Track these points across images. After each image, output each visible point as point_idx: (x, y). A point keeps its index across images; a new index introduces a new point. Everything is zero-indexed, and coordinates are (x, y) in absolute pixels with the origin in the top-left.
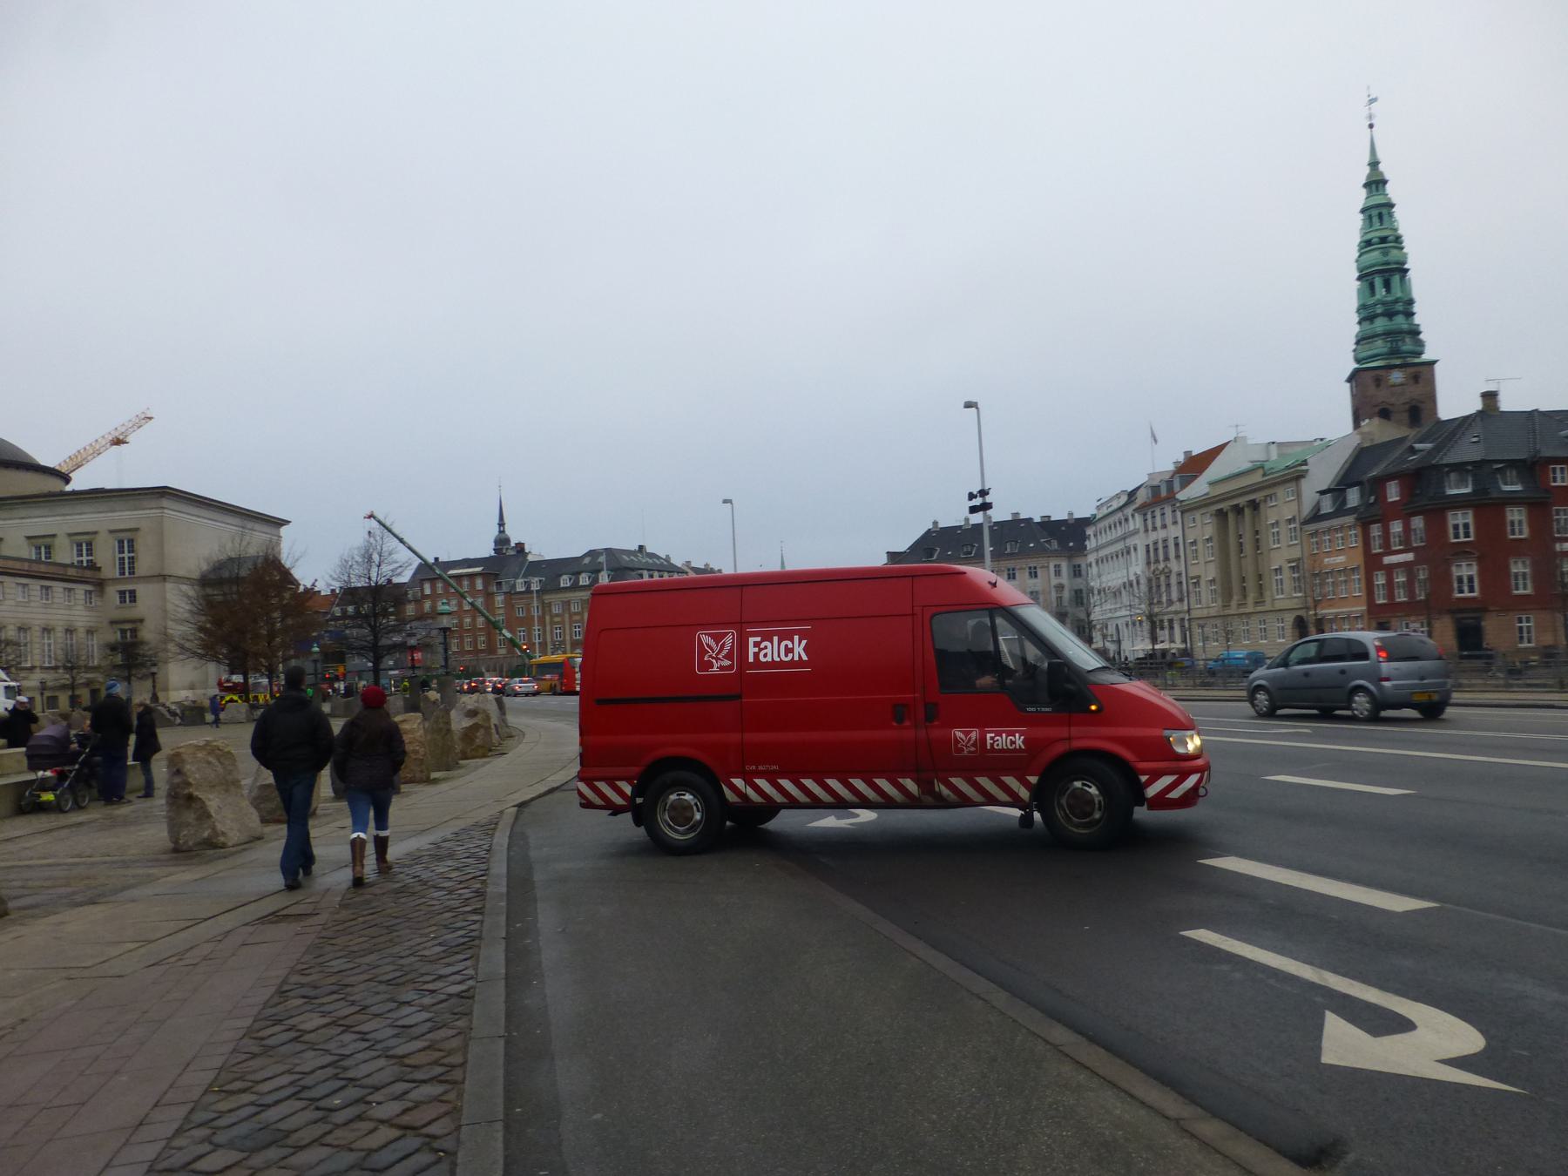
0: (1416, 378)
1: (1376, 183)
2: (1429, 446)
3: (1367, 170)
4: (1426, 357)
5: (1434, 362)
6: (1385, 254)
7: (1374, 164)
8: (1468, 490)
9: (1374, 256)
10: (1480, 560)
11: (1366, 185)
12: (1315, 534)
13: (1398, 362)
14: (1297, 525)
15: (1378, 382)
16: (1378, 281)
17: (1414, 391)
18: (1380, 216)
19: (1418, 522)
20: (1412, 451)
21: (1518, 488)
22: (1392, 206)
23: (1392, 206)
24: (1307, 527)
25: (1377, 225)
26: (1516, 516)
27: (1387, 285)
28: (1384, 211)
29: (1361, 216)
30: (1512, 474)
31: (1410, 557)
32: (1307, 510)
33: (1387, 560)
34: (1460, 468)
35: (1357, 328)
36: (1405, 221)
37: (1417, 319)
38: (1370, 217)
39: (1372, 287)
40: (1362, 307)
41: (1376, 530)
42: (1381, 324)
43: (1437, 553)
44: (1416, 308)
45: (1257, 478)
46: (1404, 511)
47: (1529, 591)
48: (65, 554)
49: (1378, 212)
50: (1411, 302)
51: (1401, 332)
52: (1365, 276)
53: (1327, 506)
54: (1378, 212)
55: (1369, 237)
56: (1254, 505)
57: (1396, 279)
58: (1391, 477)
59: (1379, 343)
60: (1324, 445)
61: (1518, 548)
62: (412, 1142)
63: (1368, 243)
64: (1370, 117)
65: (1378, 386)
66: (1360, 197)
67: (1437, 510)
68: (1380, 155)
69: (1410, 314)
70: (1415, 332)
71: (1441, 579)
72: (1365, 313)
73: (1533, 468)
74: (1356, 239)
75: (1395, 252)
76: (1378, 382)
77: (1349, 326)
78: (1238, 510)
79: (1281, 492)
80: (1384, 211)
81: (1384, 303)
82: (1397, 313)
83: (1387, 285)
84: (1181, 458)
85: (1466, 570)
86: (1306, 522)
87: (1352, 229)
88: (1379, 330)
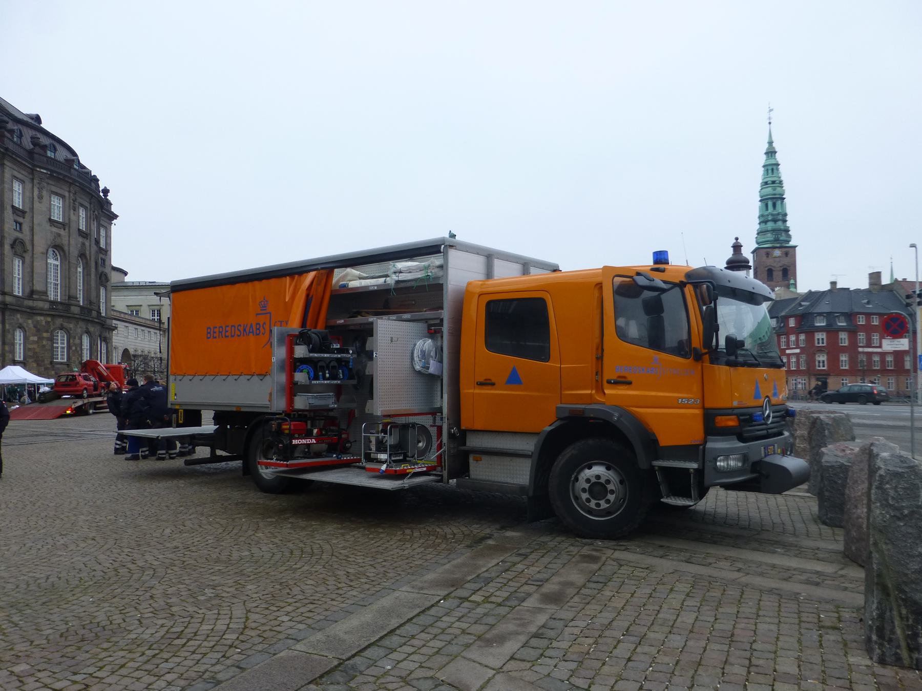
0: (787, 254)
1: (771, 153)
3: (767, 146)
4: (792, 243)
6: (774, 190)
7: (771, 143)
8: (824, 324)
9: (769, 190)
10: (828, 354)
15: (768, 254)
16: (770, 204)
17: (786, 261)
18: (772, 170)
19: (802, 337)
20: (801, 306)
21: (844, 324)
22: (778, 165)
23: (778, 165)
25: (770, 175)
26: (843, 336)
27: (774, 205)
28: (775, 167)
30: (842, 318)
31: (798, 351)
33: (788, 352)
34: (820, 314)
35: (758, 227)
36: (785, 173)
37: (788, 224)
38: (767, 170)
39: (767, 206)
40: (761, 216)
41: (783, 339)
42: (770, 225)
43: (810, 351)
44: (788, 218)
46: (797, 331)
48: (146, 314)
49: (772, 168)
50: (786, 215)
51: (780, 230)
52: (764, 200)
54: (772, 168)
57: (779, 203)
61: (844, 350)
64: (770, 118)
66: (762, 159)
67: (811, 332)
68: (774, 139)
69: (785, 221)
70: (787, 231)
71: (811, 362)
72: (762, 219)
73: (850, 316)
75: (779, 189)
76: (768, 254)
80: (775, 167)
81: (772, 215)
83: (774, 205)
85: (822, 358)
87: (758, 175)
88: (770, 228)
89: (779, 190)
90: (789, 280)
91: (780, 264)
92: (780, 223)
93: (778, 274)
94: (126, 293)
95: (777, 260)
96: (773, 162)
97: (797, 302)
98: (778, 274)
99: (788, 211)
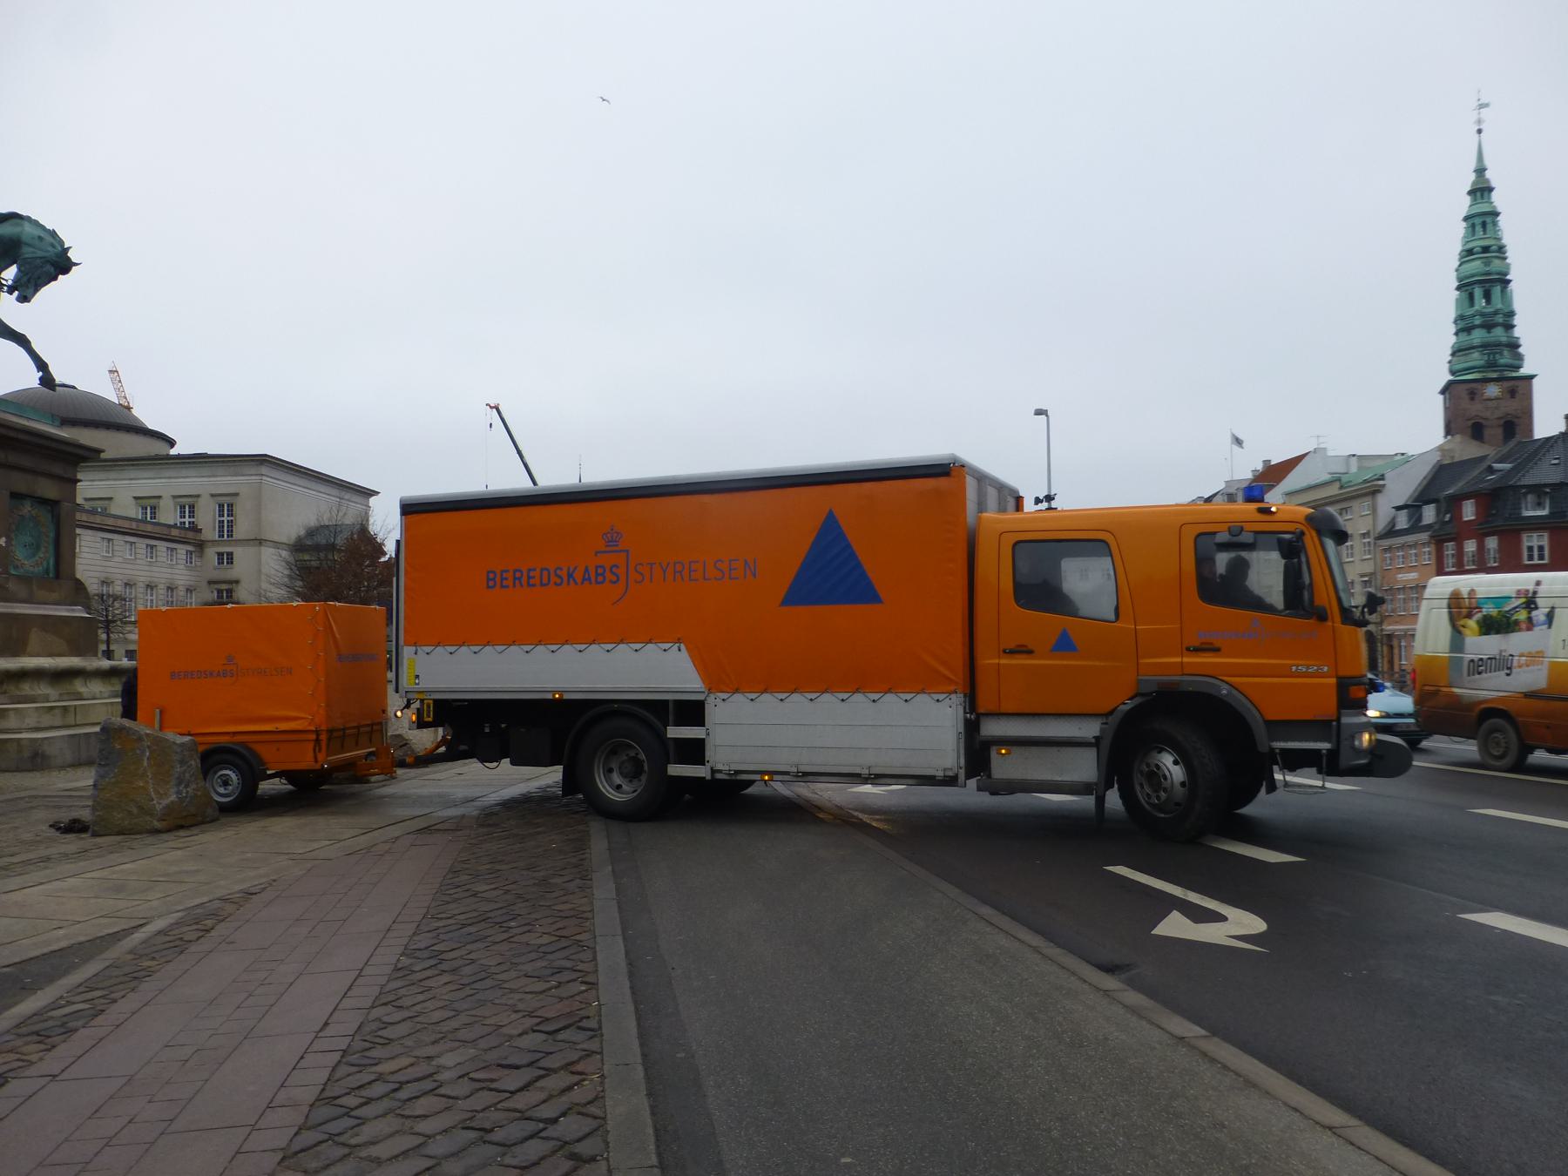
0: (1512, 393)
1: (1481, 190)
2: (1508, 466)
3: (1473, 177)
4: (1524, 371)
5: (1532, 377)
6: (1487, 264)
7: (1480, 171)
8: (1545, 512)
9: (1476, 266)
11: (1470, 193)
12: (1389, 549)
13: (1494, 375)
15: (1472, 395)
16: (1478, 292)
17: (1510, 407)
18: (1484, 225)
19: (1492, 543)
20: (1490, 470)
22: (1497, 214)
23: (1497, 214)
24: (1380, 542)
28: (1488, 220)
29: (1464, 224)
32: (1382, 525)
34: (1538, 490)
35: (1453, 339)
36: (1510, 230)
37: (1517, 332)
38: (1473, 226)
39: (1471, 297)
40: (1460, 318)
42: (1478, 336)
44: (1517, 320)
45: (1333, 490)
46: (1480, 531)
48: (169, 515)
49: (1482, 220)
50: (1511, 314)
51: (1499, 344)
52: (1465, 286)
53: (1403, 522)
54: (1482, 220)
57: (1497, 290)
58: (1467, 497)
59: (1476, 355)
60: (1404, 460)
62: (564, 943)
63: (1470, 252)
64: (1479, 122)
66: (1464, 204)
68: (1487, 162)
69: (1509, 327)
70: (1514, 346)
72: (1462, 324)
74: (1457, 247)
75: (1497, 262)
76: (1472, 395)
77: (1447, 338)
79: (1355, 504)
80: (1488, 220)
81: (1482, 315)
83: (1487, 296)
84: (1260, 467)
87: (1453, 236)
88: (1477, 342)
89: (1496, 265)
91: (1498, 414)
92: (1499, 331)
94: (133, 473)
95: (1490, 404)
96: (1484, 208)
97: (1484, 465)
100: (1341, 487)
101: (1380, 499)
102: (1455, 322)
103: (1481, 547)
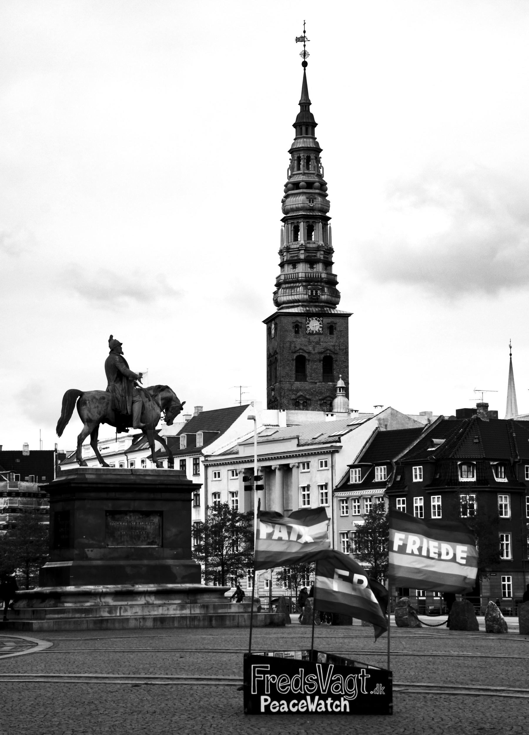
1: (305, 124)
3: (297, 110)
4: (341, 308)
5: (350, 315)
7: (305, 104)
8: (474, 479)
9: (299, 201)
12: (346, 500)
14: (330, 490)
15: (298, 328)
17: (330, 342)
18: (308, 159)
19: (436, 501)
21: (506, 480)
22: (320, 150)
23: (320, 150)
24: (338, 494)
28: (312, 156)
29: (290, 156)
32: (338, 480)
35: (278, 271)
37: (335, 270)
39: (296, 230)
42: (302, 270)
45: (292, 446)
46: (426, 490)
47: (510, 558)
50: (330, 251)
51: (321, 280)
52: (290, 219)
53: (355, 478)
55: (295, 179)
56: (287, 470)
65: (297, 332)
68: (311, 97)
69: (328, 264)
70: (332, 282)
74: (283, 179)
78: (268, 471)
81: (307, 250)
82: (317, 261)
86: (338, 489)
90: (334, 380)
92: (319, 267)
93: (314, 368)
95: (312, 338)
96: (309, 143)
98: (314, 368)
99: (335, 244)
100: (298, 445)
101: (337, 456)
102: (281, 253)
103: (427, 503)
